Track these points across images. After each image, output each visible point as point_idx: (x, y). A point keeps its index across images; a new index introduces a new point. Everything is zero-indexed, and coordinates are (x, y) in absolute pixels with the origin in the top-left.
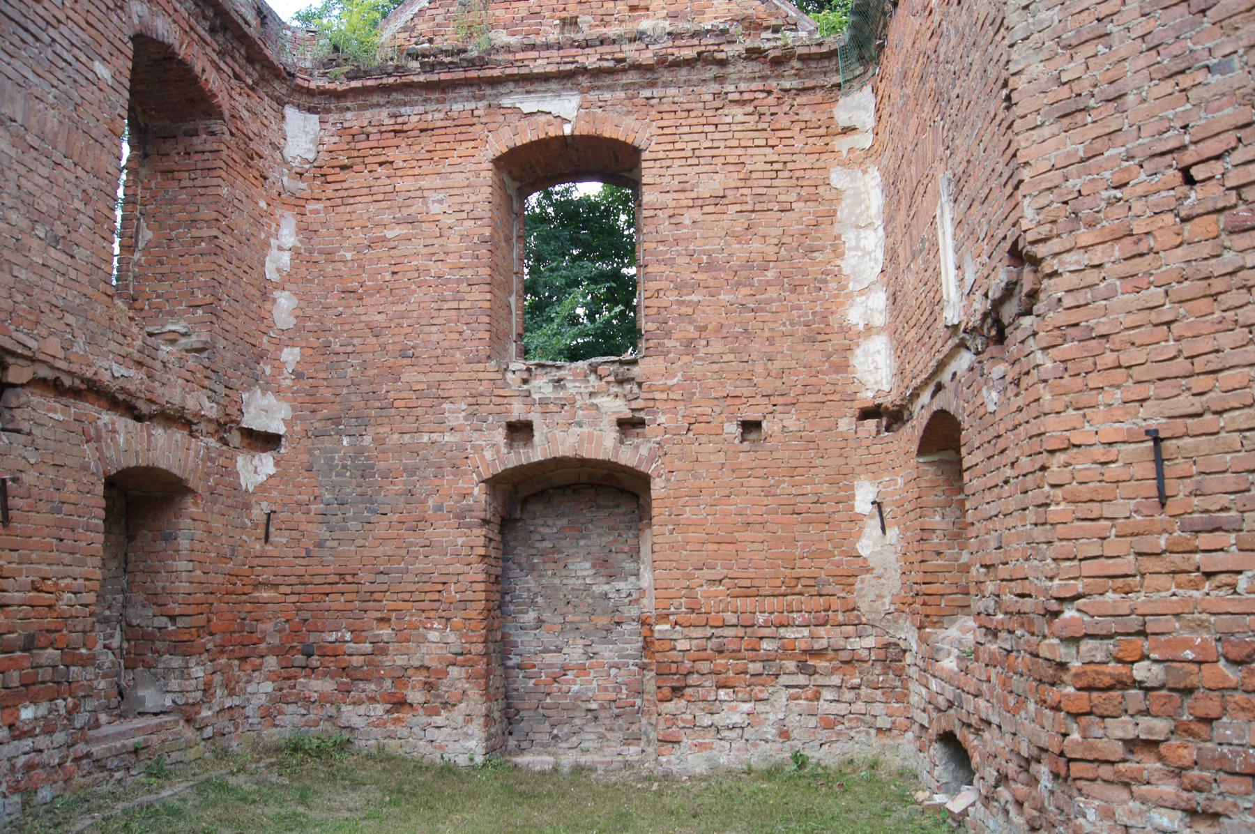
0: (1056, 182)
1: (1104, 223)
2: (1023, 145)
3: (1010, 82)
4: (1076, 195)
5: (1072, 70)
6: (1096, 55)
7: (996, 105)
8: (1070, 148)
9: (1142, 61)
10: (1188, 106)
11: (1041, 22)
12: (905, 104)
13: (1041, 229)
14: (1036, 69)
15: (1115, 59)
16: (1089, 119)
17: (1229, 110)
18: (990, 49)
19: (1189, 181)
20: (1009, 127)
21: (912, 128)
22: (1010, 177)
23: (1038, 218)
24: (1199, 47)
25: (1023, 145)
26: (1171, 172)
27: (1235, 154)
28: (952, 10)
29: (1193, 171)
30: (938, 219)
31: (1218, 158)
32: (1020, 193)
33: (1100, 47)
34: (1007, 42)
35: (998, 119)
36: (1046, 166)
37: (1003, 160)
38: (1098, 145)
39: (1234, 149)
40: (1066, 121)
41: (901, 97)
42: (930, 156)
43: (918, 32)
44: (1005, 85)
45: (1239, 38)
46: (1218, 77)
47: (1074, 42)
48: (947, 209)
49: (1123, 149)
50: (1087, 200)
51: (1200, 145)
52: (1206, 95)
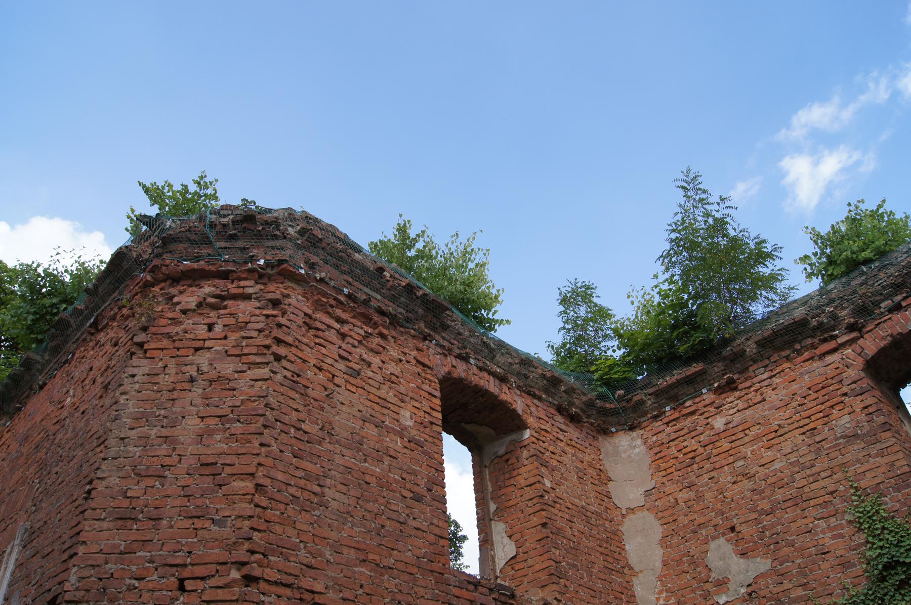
0: (99, 563)
1: (121, 602)
2: (87, 528)
3: (94, 483)
4: (109, 576)
5: (136, 490)
6: (153, 487)
7: (79, 493)
8: (117, 542)
9: (178, 502)
10: (195, 540)
11: (128, 452)
12: (18, 458)
13: (77, 593)
14: (114, 481)
15: (163, 494)
16: (135, 527)
17: (216, 551)
18: (90, 454)
19: (182, 588)
20: (82, 512)
21: (16, 477)
22: (70, 548)
23: (78, 584)
24: (212, 506)
25: (87, 528)
26: (173, 579)
27: (213, 579)
28: (76, 414)
29: (186, 583)
30: (6, 555)
31: (203, 579)
32: (74, 561)
33: (157, 483)
34: (102, 455)
35: (77, 503)
36: (95, 548)
37: (70, 533)
38: (135, 546)
39: (213, 576)
40: (120, 522)
41: (17, 452)
42: (19, 504)
43: (48, 415)
44: (90, 483)
45: (234, 509)
46: (217, 527)
47: (143, 473)
48: (16, 550)
49: (149, 554)
50: (116, 582)
51: (195, 567)
52: (207, 537)
